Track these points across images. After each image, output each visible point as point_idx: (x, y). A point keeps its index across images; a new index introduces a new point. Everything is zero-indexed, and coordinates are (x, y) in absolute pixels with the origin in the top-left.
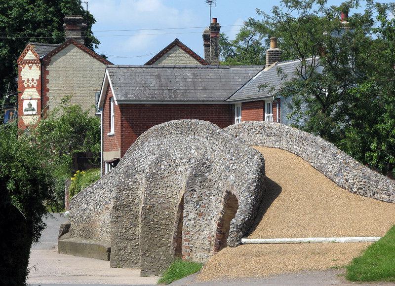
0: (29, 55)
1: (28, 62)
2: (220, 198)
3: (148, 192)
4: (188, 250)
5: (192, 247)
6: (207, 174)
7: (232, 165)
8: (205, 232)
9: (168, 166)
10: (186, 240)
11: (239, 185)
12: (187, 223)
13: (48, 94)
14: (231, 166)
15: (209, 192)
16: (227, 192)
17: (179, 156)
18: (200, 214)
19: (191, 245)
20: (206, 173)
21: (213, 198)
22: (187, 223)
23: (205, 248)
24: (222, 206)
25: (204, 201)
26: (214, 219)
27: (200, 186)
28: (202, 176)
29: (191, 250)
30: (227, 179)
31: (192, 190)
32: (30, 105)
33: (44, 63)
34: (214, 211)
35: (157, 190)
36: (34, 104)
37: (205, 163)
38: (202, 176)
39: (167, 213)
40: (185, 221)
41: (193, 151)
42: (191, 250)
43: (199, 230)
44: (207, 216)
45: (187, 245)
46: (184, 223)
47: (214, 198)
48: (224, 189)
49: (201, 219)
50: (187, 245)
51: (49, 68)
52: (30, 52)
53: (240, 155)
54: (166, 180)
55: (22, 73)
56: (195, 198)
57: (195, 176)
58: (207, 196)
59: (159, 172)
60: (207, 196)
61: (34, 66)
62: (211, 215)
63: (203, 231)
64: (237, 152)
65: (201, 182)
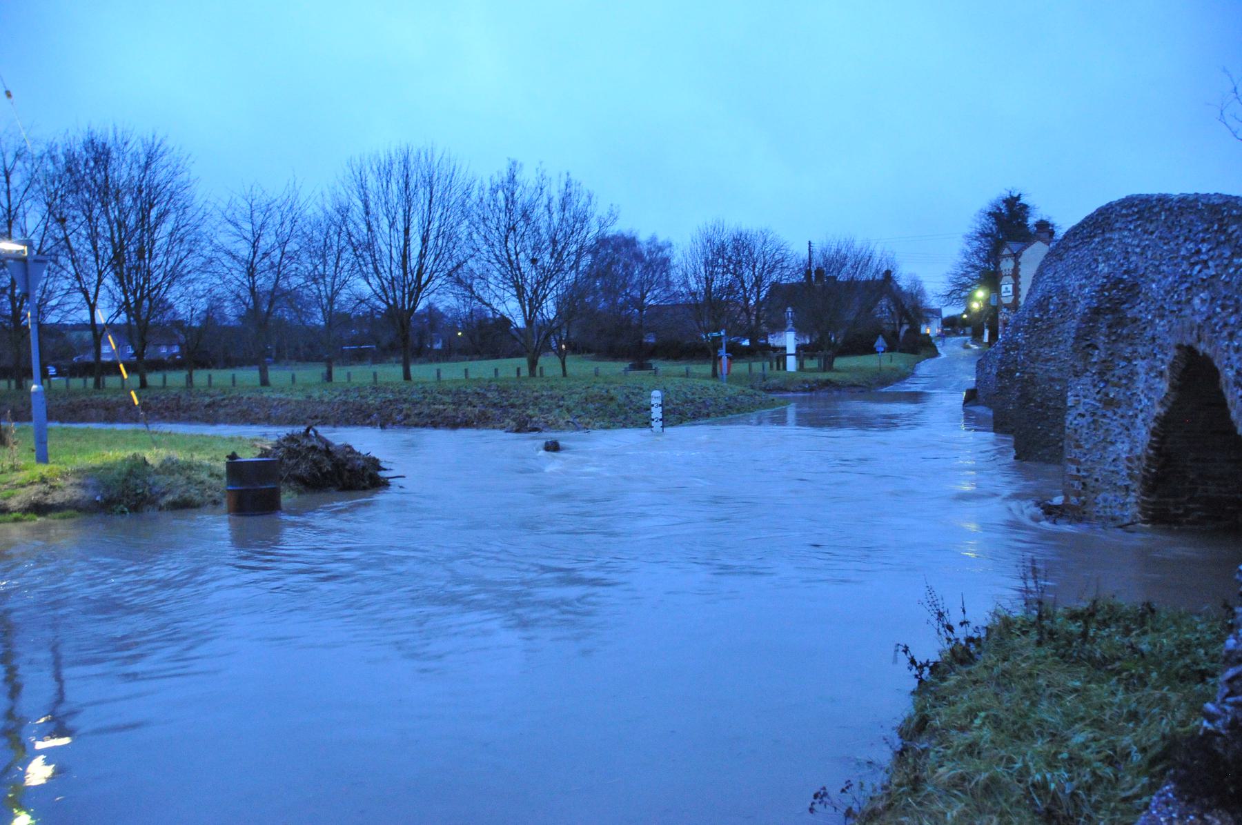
0: (1006, 252)
1: (1005, 256)
2: (1159, 363)
3: (1026, 352)
4: (1076, 483)
5: (1084, 477)
6: (1126, 306)
7: (1197, 268)
8: (1119, 446)
9: (1061, 305)
10: (1072, 461)
11: (1226, 325)
12: (1076, 422)
13: (1020, 280)
14: (1195, 272)
15: (1130, 349)
16: (1179, 347)
17: (1077, 283)
18: (1109, 403)
19: (1085, 474)
20: (1124, 303)
21: (1141, 365)
22: (1076, 422)
23: (1119, 484)
24: (1164, 386)
25: (1118, 372)
26: (1141, 416)
27: (1108, 336)
28: (1114, 310)
29: (1084, 484)
30: (1180, 310)
31: (1089, 346)
32: (1007, 288)
33: (1016, 256)
34: (1142, 397)
35: (1042, 347)
36: (1010, 287)
37: (1121, 281)
38: (1114, 310)
39: (1058, 388)
40: (1070, 418)
41: (1101, 266)
42: (1084, 484)
43: (1104, 440)
44: (1124, 407)
45: (1075, 473)
46: (1068, 423)
47: (1143, 363)
48: (1172, 340)
49: (1109, 414)
50: (1075, 473)
51: (1020, 260)
52: (1006, 249)
53: (1230, 230)
54: (1056, 330)
55: (1001, 265)
56: (1096, 362)
57: (1097, 311)
58: (1126, 359)
59: (1045, 317)
60: (1126, 359)
61: (1010, 259)
62: (1136, 404)
63: (1112, 443)
64: (1216, 227)
65: (1110, 327)
